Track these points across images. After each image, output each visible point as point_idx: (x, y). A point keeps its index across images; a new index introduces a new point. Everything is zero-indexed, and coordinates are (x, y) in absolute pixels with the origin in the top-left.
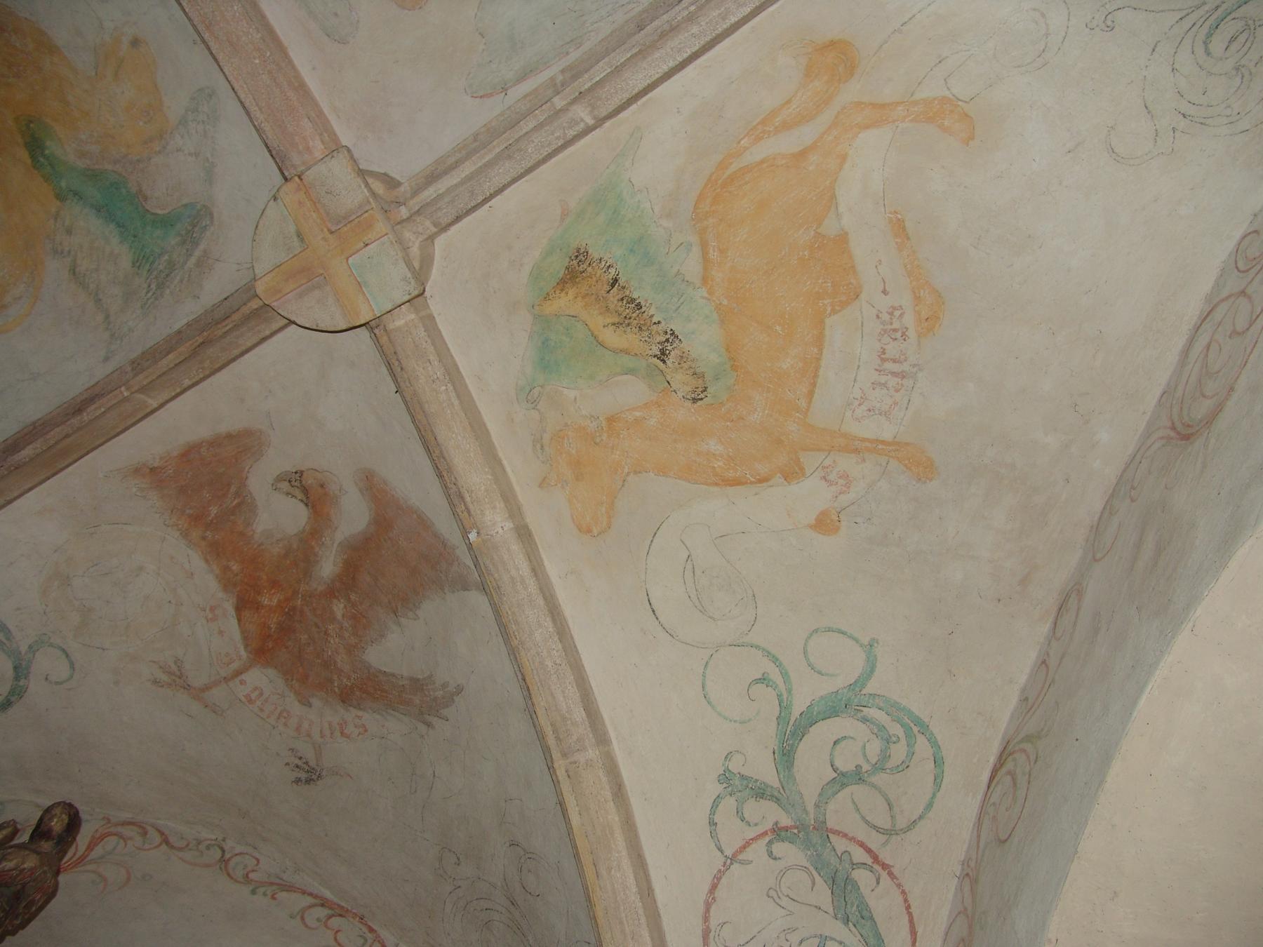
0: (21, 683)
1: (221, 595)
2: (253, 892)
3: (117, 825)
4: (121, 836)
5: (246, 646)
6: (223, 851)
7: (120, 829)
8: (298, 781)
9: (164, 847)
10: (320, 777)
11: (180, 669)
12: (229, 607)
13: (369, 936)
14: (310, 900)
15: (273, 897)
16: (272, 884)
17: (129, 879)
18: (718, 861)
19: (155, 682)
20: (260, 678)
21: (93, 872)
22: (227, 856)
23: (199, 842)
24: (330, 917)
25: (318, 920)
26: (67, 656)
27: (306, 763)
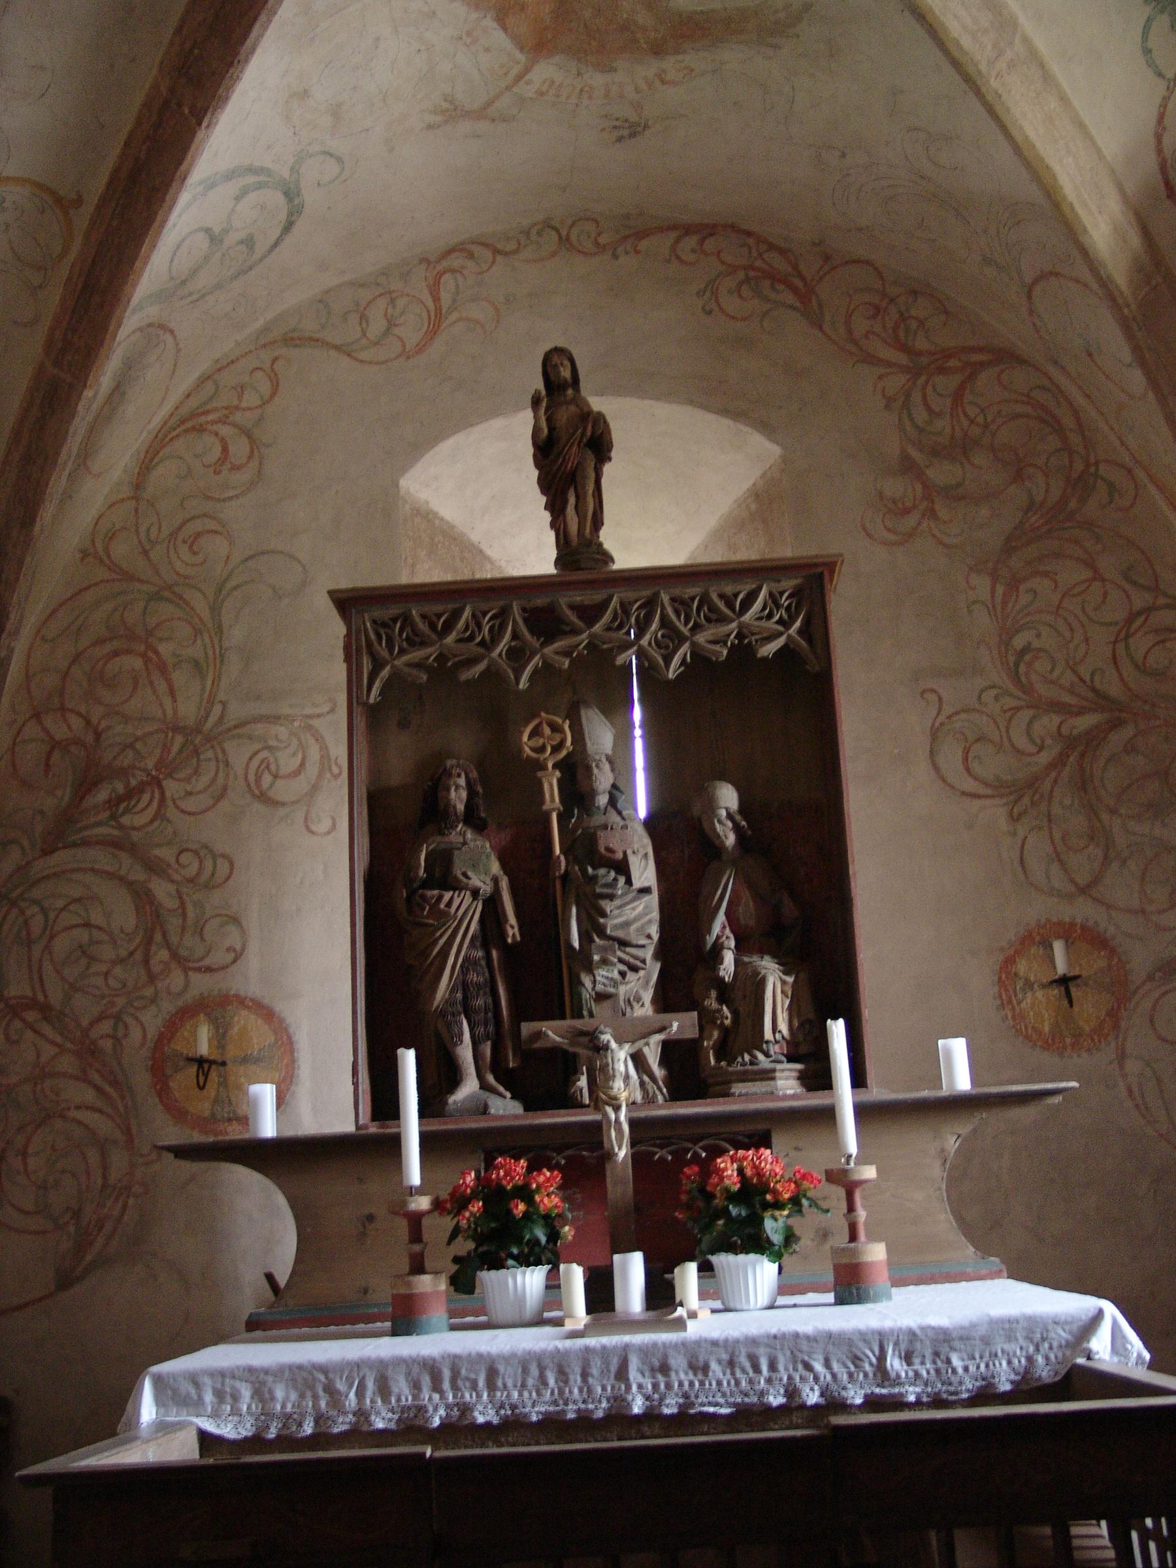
0: (296, 202)
1: (474, 15)
2: (615, 257)
3: (439, 261)
4: (453, 271)
5: (522, 50)
6: (558, 231)
7: (445, 263)
8: (620, 139)
9: (499, 259)
10: (646, 127)
11: (451, 103)
12: (489, 23)
13: (751, 241)
14: (673, 235)
15: (637, 252)
16: (625, 238)
17: (497, 310)
18: (1161, 88)
19: (430, 127)
20: (546, 71)
22: (564, 233)
23: (527, 233)
24: (702, 242)
25: (693, 251)
26: (331, 155)
27: (626, 121)
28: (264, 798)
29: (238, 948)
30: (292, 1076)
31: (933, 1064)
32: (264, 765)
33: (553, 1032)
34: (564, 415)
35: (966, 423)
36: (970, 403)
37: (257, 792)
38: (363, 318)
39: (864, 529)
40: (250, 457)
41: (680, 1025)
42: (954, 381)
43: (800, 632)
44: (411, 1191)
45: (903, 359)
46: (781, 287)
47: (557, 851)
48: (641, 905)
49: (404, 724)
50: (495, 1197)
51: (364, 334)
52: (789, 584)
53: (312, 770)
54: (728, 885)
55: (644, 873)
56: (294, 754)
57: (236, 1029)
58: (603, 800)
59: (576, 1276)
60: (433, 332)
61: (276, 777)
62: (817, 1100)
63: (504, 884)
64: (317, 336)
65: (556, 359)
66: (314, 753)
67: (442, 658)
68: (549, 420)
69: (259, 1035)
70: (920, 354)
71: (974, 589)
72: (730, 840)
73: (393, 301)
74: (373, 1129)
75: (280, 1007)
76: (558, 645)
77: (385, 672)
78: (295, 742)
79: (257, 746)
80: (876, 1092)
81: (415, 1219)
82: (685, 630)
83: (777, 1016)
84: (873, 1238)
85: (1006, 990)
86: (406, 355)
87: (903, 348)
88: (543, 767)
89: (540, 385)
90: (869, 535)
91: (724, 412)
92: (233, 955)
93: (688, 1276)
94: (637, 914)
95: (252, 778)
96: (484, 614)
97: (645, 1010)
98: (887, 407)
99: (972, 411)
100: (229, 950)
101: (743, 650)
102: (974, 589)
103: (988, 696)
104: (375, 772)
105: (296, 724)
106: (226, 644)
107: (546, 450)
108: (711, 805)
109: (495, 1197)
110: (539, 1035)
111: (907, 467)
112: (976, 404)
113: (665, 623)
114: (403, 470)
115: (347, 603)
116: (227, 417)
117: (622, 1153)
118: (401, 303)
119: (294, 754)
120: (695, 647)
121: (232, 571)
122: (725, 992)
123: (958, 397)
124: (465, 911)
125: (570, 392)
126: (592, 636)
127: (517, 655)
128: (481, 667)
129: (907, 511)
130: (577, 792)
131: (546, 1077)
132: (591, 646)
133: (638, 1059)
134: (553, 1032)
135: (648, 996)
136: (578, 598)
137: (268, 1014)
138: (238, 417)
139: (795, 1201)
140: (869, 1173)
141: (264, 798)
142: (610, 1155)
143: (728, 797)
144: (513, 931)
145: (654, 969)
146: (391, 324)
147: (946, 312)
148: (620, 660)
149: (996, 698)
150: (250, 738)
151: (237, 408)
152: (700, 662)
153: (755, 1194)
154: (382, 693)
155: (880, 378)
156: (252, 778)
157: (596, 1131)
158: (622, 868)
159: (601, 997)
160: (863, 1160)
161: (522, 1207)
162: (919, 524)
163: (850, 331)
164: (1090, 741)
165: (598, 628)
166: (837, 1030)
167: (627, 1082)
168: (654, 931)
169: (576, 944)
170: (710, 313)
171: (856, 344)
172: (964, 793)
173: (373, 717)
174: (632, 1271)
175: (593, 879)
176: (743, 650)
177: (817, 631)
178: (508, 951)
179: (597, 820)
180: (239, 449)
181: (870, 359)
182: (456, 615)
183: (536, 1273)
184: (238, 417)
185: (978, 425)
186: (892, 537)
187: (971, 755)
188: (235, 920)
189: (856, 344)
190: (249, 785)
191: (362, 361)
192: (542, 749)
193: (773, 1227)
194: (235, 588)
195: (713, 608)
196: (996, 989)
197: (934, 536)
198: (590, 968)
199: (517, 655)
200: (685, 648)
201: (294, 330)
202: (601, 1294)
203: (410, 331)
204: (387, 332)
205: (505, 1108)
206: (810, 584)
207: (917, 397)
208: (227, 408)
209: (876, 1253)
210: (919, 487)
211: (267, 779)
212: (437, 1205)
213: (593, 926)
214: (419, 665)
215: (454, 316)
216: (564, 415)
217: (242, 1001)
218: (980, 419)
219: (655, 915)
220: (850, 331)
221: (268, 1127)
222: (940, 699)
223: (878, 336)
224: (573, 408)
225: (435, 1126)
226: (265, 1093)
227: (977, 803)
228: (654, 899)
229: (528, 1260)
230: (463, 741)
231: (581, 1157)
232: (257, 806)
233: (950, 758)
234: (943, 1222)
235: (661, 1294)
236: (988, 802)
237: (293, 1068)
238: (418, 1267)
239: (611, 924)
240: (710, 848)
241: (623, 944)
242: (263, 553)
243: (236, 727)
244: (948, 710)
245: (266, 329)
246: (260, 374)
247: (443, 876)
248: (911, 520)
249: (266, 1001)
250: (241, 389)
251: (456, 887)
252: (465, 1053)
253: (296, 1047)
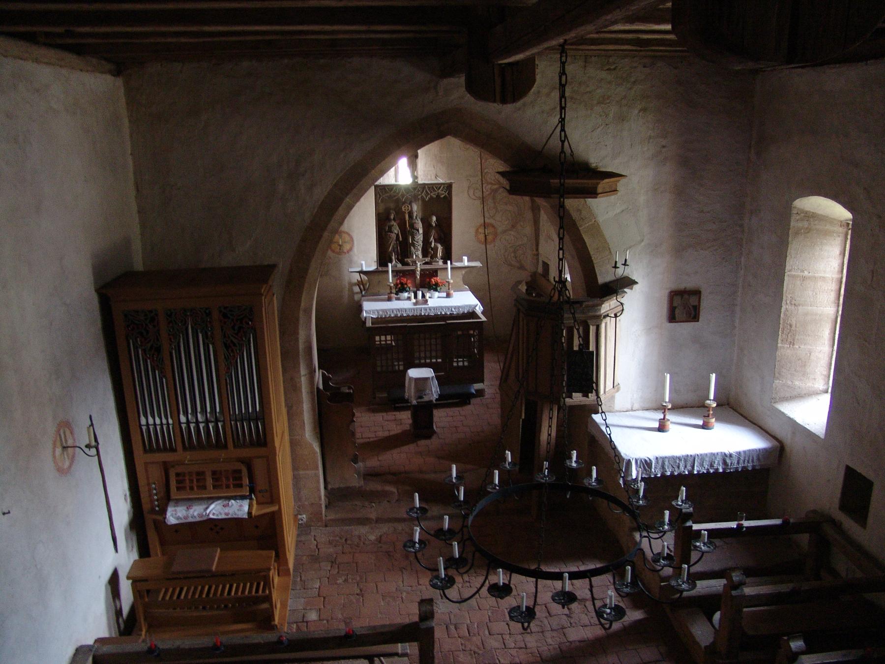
50: (402, 284)
55: (421, 231)
69: (347, 238)
83: (440, 253)
94: (420, 237)
101: (438, 196)
122: (432, 249)
124: (394, 236)
130: (411, 216)
137: (349, 235)
143: (434, 218)
153: (437, 285)
157: (413, 272)
164: (495, 191)
177: (450, 193)
178: (400, 242)
206: (449, 187)
240: (431, 225)
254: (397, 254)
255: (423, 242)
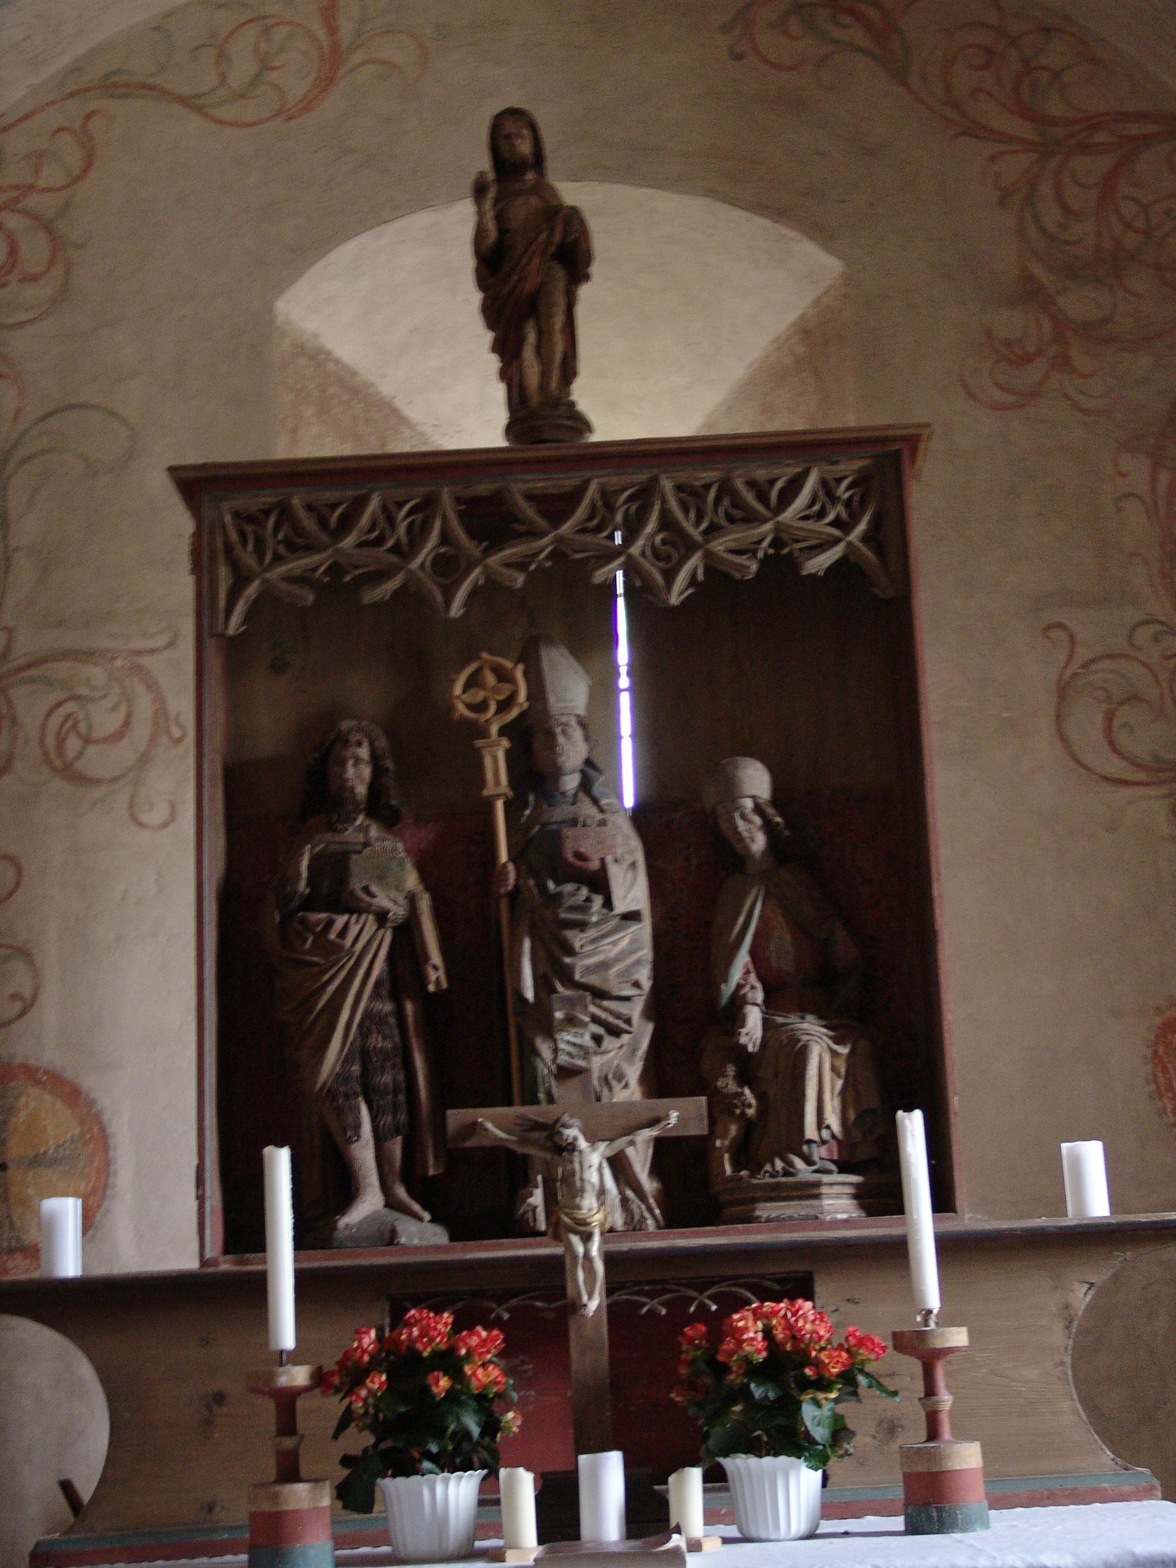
21: (366, 62)
28: (69, 772)
29: (27, 993)
30: (106, 1186)
31: (1053, 1180)
32: (69, 724)
33: (494, 1124)
34: (522, 209)
35: (1118, 228)
36: (1125, 197)
37: (58, 763)
38: (222, 56)
39: (965, 386)
40: (51, 263)
41: (681, 1115)
42: (1105, 162)
43: (866, 538)
44: (282, 1358)
45: (1025, 130)
46: (847, 20)
47: (503, 856)
48: (625, 938)
49: (278, 667)
50: (406, 1367)
51: (223, 79)
52: (850, 467)
53: (141, 732)
54: (754, 911)
55: (631, 890)
56: (114, 708)
57: (22, 1116)
58: (571, 782)
59: (523, 1487)
60: (325, 82)
61: (87, 741)
62: (882, 1228)
63: (425, 904)
64: (150, 81)
65: (510, 127)
66: (144, 705)
67: (336, 570)
68: (500, 217)
69: (56, 1124)
70: (1054, 122)
71: (1124, 475)
72: (759, 843)
73: (266, 31)
74: (226, 1266)
75: (89, 1083)
76: (510, 552)
77: (252, 590)
78: (116, 689)
79: (59, 695)
80: (970, 1218)
81: (287, 1400)
82: (696, 533)
84: (963, 1435)
85: (1165, 1070)
86: (286, 113)
87: (1025, 112)
88: (483, 733)
89: (483, 163)
90: (971, 395)
91: (761, 208)
92: (18, 1006)
93: (689, 1488)
94: (621, 950)
95: (50, 741)
96: (400, 505)
97: (629, 1092)
98: (1002, 203)
99: (1128, 209)
100: (14, 997)
101: (781, 564)
102: (1124, 475)
103: (1144, 635)
104: (235, 736)
105: (118, 663)
106: (14, 543)
107: (493, 262)
108: (730, 791)
109: (406, 1367)
110: (473, 1128)
111: (1030, 293)
112: (1135, 200)
113: (667, 523)
114: (281, 287)
115: (196, 485)
116: (16, 200)
117: (594, 1304)
118: (280, 33)
119: (114, 708)
120: (709, 555)
121: (24, 433)
122: (748, 1067)
123: (1107, 187)
124: (366, 943)
125: (530, 176)
126: (559, 540)
127: (448, 567)
128: (394, 583)
129: (1027, 359)
131: (484, 1190)
132: (556, 555)
133: (619, 1165)
134: (494, 1124)
135: (634, 1072)
136: (540, 483)
137: (72, 1094)
138: (33, 201)
139: (848, 1378)
140: (958, 1337)
141: (69, 772)
142: (576, 1307)
143: (756, 780)
144: (436, 975)
145: (643, 1033)
146: (265, 66)
147: (1093, 60)
148: (599, 576)
149: (1156, 639)
150: (49, 682)
151: (31, 187)
152: (716, 578)
153: (789, 1366)
154: (248, 619)
155: (993, 158)
156: (50, 741)
157: (554, 1272)
158: (599, 883)
159: (566, 1073)
160: (948, 1318)
161: (444, 1383)
162: (1046, 376)
163: (948, 88)
165: (566, 528)
166: (913, 1127)
167: (602, 1197)
168: (644, 975)
169: (529, 994)
170: (739, 57)
171: (955, 105)
172: (1106, 779)
173: (233, 655)
174: (607, 1479)
175: (556, 899)
176: (781, 564)
177: (890, 537)
178: (430, 1004)
179: (562, 812)
180: (35, 250)
181: (977, 130)
182: (360, 504)
183: (464, 1483)
184: (33, 201)
185: (1137, 231)
186: (1004, 397)
187: (1116, 723)
188: (25, 953)
189: (955, 105)
190: (46, 754)
191: (221, 122)
192: (481, 707)
193: (814, 1416)
194: (27, 459)
195: (738, 502)
196: (1149, 1067)
197: (1066, 395)
198: (549, 1031)
199: (448, 567)
200: (694, 563)
201: (117, 72)
202: (560, 1513)
203: (294, 81)
204: (257, 79)
205: (422, 1235)
206: (880, 469)
207: (1046, 189)
208: (16, 187)
209: (967, 1457)
210: (1046, 324)
211: (73, 745)
212: (320, 1379)
213: (555, 967)
214: (301, 580)
215: (358, 57)
216: (522, 209)
217: (32, 1074)
218: (1140, 223)
219: (646, 953)
220: (948, 88)
221: (69, 1263)
222: (1072, 637)
223: (990, 95)
224: (534, 201)
225: (320, 1261)
226: (66, 1211)
227: (1126, 792)
228: (644, 930)
229: (453, 1463)
230: (366, 692)
231: (532, 1309)
232: (58, 784)
233: (1087, 723)
234: (1067, 1413)
235: (648, 1514)
236: (1141, 791)
237: (108, 1175)
238: (290, 1472)
239: (580, 967)
240: (727, 855)
241: (600, 994)
242: (72, 407)
243: (28, 666)
244: (1083, 654)
245: (76, 69)
246: (66, 137)
247: (335, 891)
248: (1033, 373)
249: (69, 1074)
250: (38, 159)
251: (354, 908)
252: (364, 1153)
253: (112, 1142)
254: (408, 1128)
255: (656, 1008)
